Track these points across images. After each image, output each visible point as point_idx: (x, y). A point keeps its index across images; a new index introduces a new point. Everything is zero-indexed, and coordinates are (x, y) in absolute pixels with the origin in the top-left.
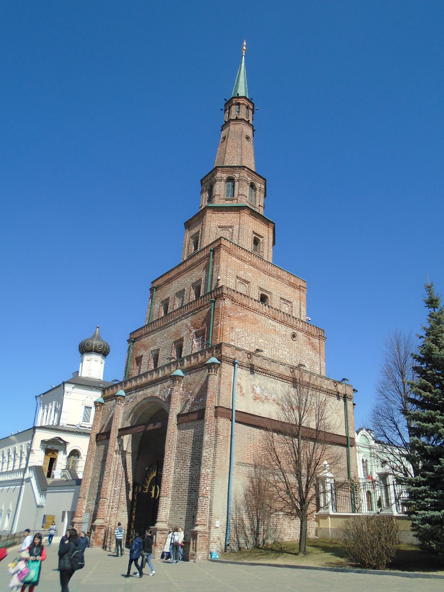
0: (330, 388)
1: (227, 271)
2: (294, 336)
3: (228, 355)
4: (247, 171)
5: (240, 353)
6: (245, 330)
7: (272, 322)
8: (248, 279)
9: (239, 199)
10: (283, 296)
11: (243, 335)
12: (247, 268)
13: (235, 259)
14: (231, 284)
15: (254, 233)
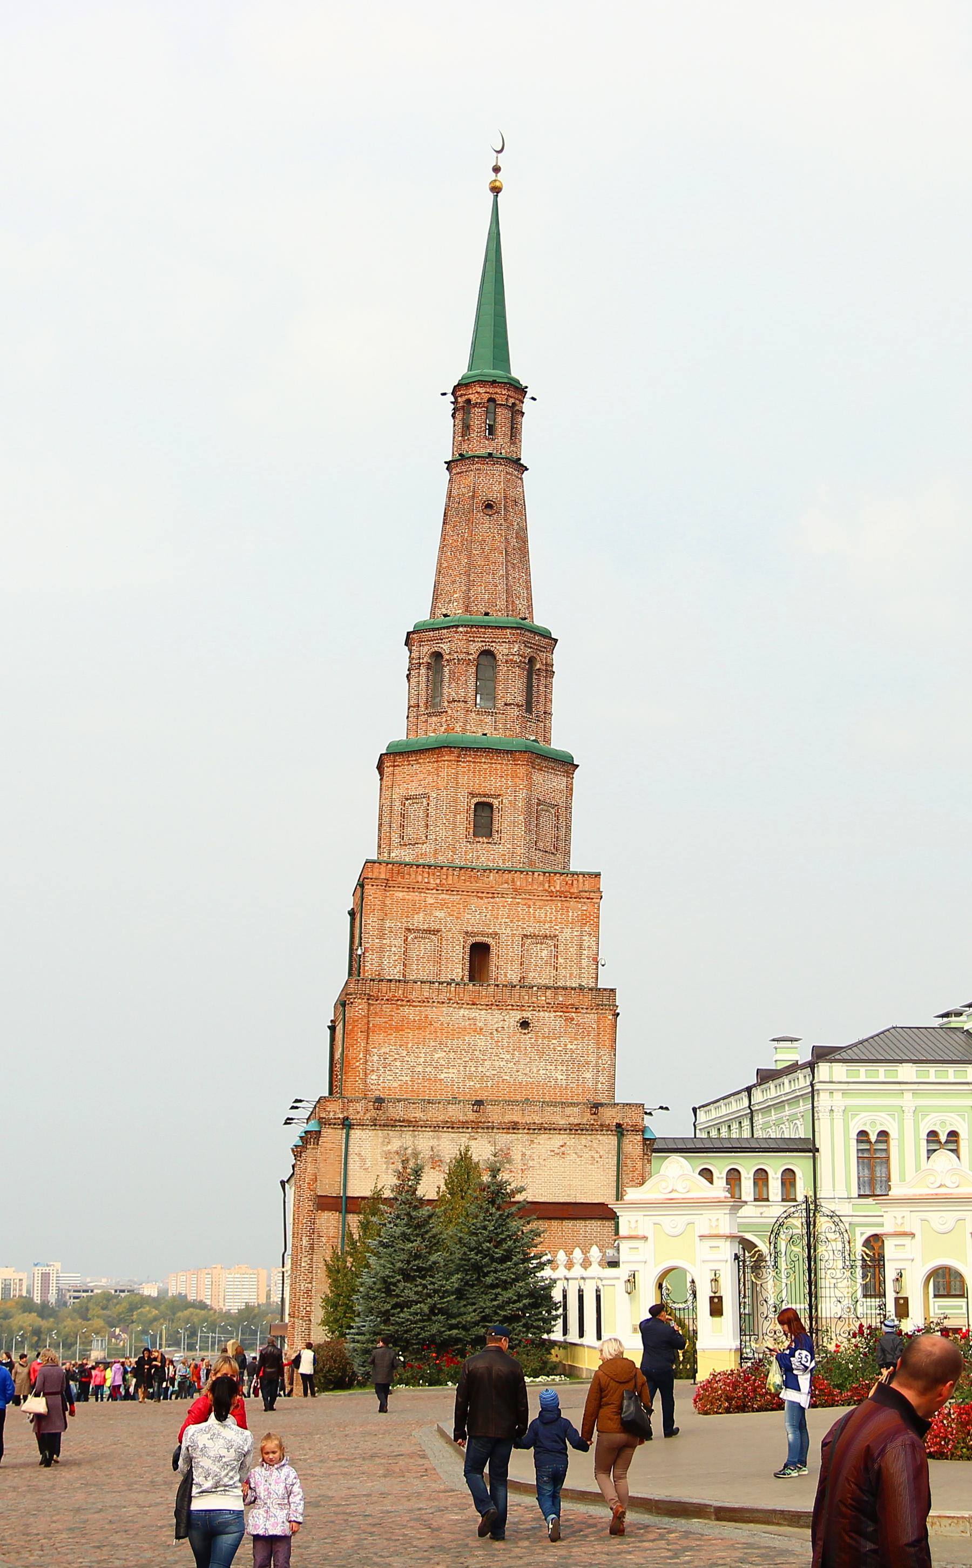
0: (576, 1122)
1: (382, 929)
2: (525, 1024)
3: (332, 1114)
4: (467, 632)
5: (359, 1106)
6: (401, 1046)
7: (467, 1012)
8: (434, 926)
9: (450, 712)
10: (530, 931)
11: (397, 1056)
12: (432, 901)
13: (400, 895)
14: (393, 949)
15: (473, 795)
